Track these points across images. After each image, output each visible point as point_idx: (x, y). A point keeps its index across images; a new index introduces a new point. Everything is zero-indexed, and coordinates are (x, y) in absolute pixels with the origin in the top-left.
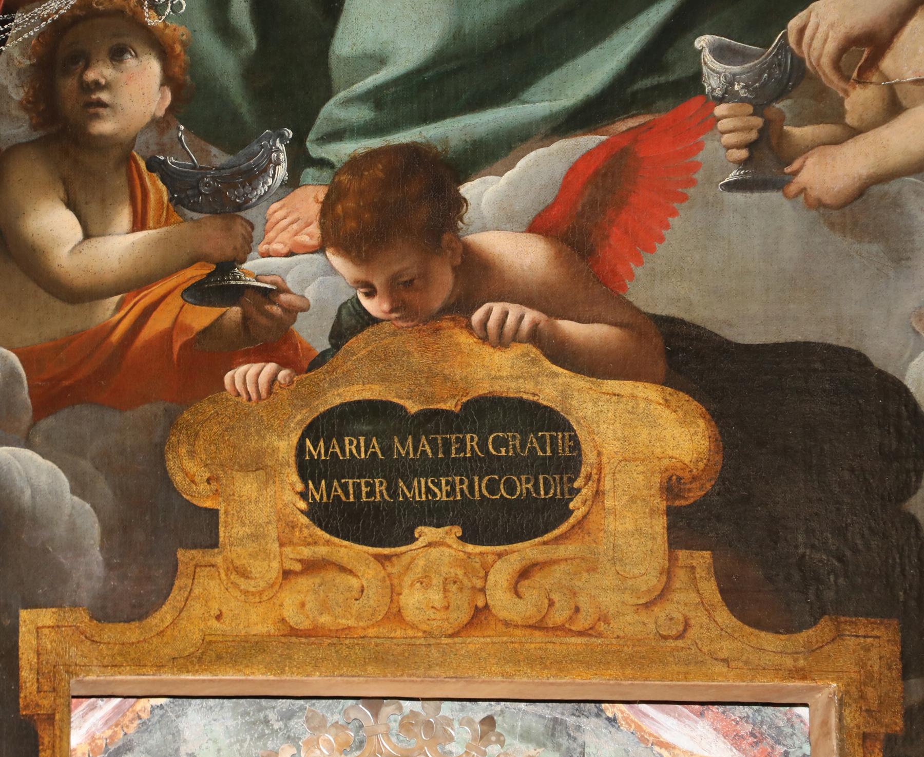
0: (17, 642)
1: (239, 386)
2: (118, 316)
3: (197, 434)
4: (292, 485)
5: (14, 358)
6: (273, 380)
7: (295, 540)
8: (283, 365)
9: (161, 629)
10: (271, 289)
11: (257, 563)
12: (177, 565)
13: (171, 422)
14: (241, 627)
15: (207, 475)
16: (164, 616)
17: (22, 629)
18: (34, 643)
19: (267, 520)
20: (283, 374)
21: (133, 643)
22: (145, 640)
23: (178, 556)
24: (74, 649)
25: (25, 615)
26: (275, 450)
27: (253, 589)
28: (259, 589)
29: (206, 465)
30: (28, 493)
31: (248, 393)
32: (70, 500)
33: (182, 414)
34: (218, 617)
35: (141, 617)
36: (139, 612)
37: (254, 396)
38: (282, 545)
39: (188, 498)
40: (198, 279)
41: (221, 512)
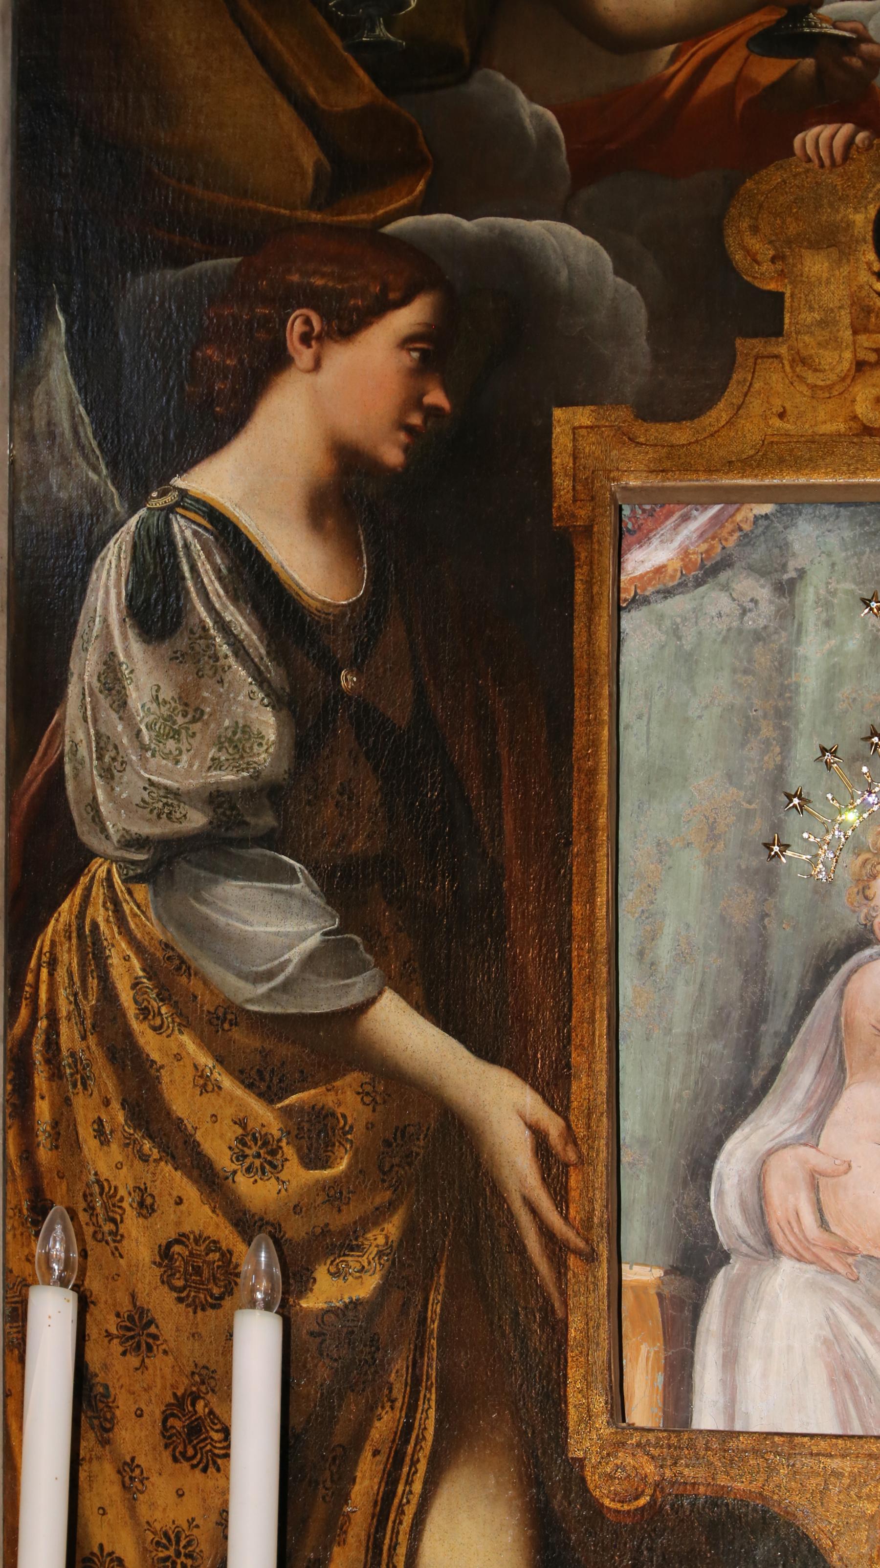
0: (550, 444)
1: (810, 150)
2: (673, 69)
3: (761, 206)
4: (869, 264)
5: (550, 115)
6: (849, 143)
7: (871, 327)
8: (861, 125)
9: (716, 429)
10: (850, 39)
11: (826, 353)
12: (735, 356)
13: (732, 191)
14: (807, 426)
15: (772, 253)
16: (719, 414)
17: (557, 430)
18: (570, 445)
19: (839, 305)
20: (861, 136)
21: (683, 445)
22: (697, 441)
23: (737, 346)
24: (615, 452)
25: (558, 413)
26: (850, 225)
27: (822, 383)
28: (828, 382)
29: (771, 242)
30: (564, 274)
31: (820, 158)
32: (613, 280)
33: (744, 182)
34: (782, 415)
35: (692, 416)
36: (692, 407)
37: (827, 162)
38: (855, 332)
39: (749, 279)
40: (766, 26)
41: (788, 295)
